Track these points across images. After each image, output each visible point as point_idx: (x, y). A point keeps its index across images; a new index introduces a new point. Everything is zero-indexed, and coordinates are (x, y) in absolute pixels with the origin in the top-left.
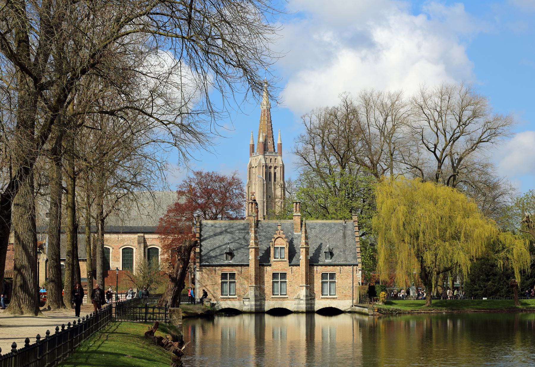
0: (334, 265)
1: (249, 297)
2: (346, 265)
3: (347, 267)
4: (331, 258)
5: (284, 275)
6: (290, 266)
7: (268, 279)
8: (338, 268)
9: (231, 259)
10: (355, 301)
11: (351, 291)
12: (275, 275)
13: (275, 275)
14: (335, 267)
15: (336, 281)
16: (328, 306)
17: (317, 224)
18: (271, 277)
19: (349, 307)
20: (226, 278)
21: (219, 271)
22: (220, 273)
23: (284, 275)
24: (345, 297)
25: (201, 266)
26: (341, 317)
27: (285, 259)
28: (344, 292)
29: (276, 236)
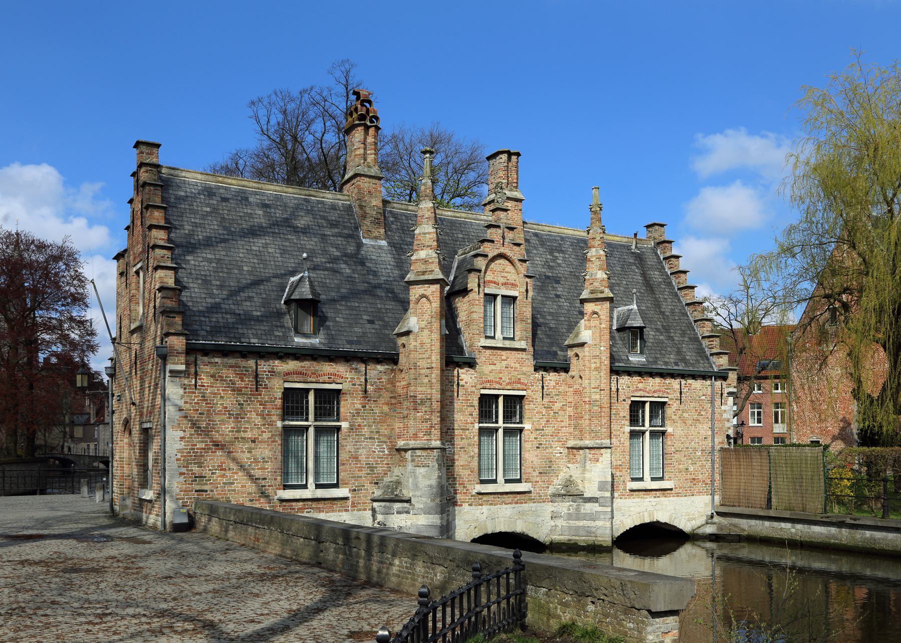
0: (662, 375)
1: (406, 493)
2: (694, 377)
3: (697, 384)
4: (642, 353)
5: (514, 404)
6: (537, 369)
7: (466, 417)
8: (675, 383)
9: (315, 333)
10: (717, 498)
11: (709, 464)
12: (487, 403)
13: (487, 403)
14: (668, 381)
15: (669, 429)
16: (647, 520)
17: (562, 239)
18: (476, 413)
19: (703, 520)
20: (302, 413)
21: (281, 375)
22: (277, 387)
23: (514, 404)
24: (691, 487)
25: (190, 350)
26: (686, 551)
27: (522, 344)
28: (691, 469)
29: (491, 250)
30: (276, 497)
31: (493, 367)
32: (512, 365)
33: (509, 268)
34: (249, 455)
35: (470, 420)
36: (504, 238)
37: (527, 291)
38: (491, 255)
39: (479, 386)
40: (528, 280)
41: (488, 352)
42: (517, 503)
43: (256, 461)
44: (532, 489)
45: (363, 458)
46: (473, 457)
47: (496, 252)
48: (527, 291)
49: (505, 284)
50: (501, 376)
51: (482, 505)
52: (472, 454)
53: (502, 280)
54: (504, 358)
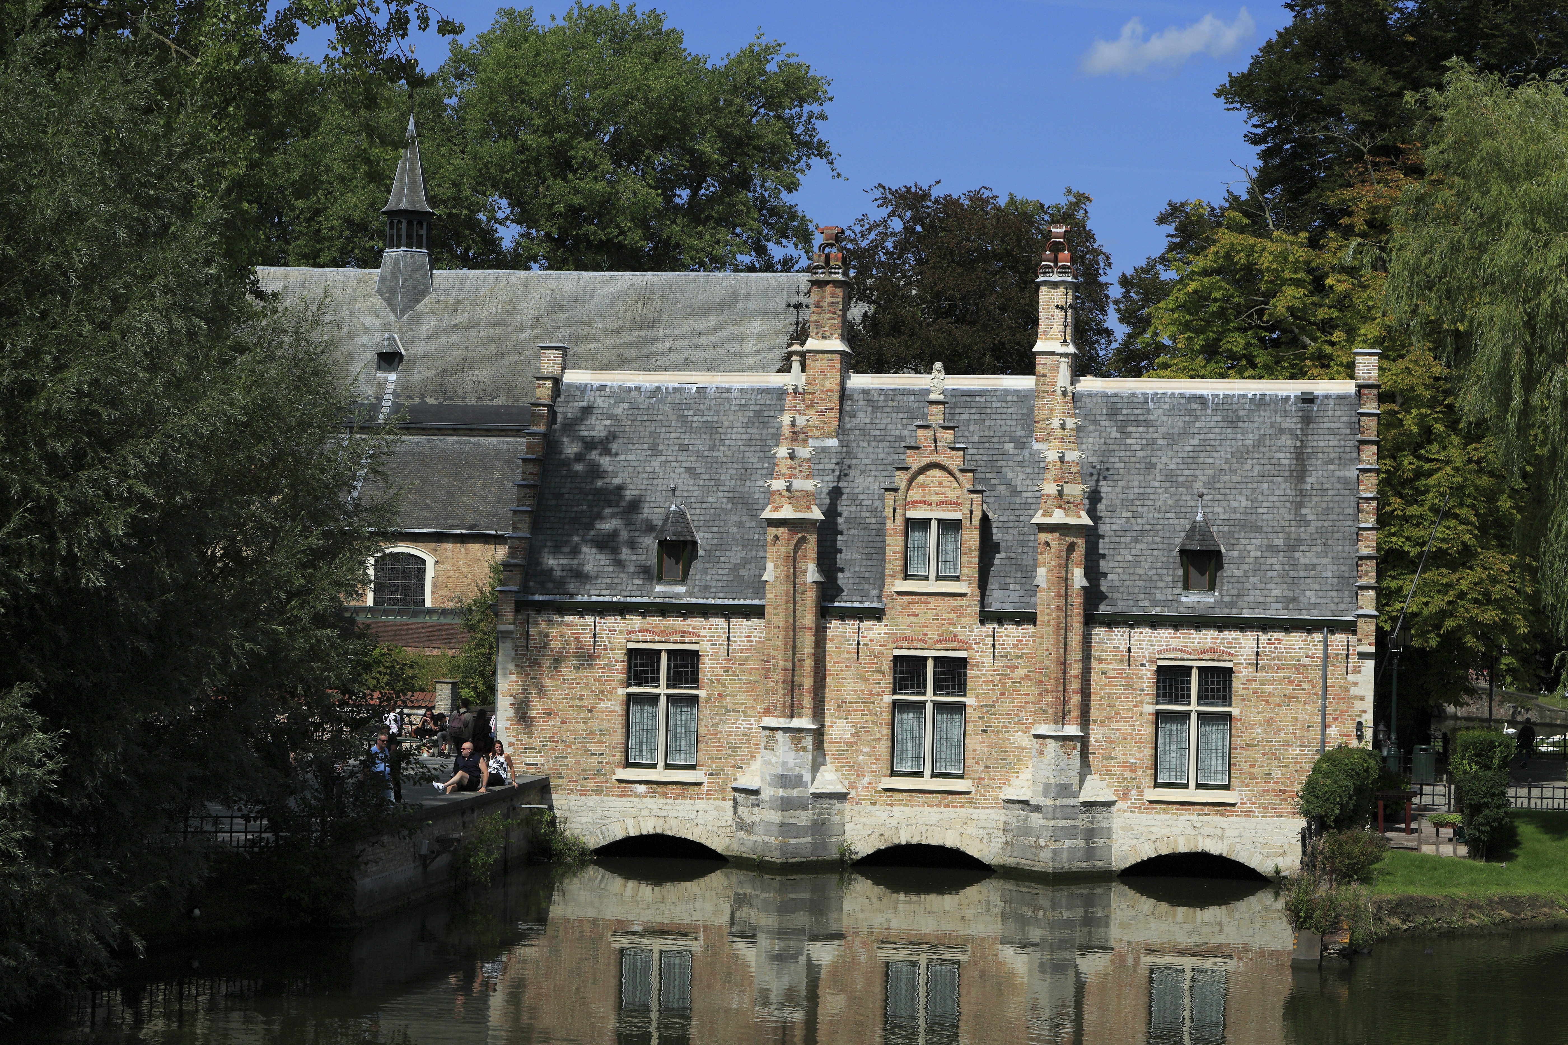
30: (615, 777)
31: (913, 619)
32: (945, 615)
33: (949, 481)
34: (584, 726)
35: (876, 690)
36: (935, 441)
37: (971, 512)
38: (915, 467)
39: (891, 646)
40: (975, 497)
41: (906, 599)
42: (947, 806)
43: (592, 734)
44: (973, 789)
45: (723, 735)
46: (879, 740)
47: (924, 462)
48: (971, 512)
49: (942, 503)
50: (925, 630)
51: (891, 805)
52: (878, 736)
53: (935, 498)
54: (930, 606)
